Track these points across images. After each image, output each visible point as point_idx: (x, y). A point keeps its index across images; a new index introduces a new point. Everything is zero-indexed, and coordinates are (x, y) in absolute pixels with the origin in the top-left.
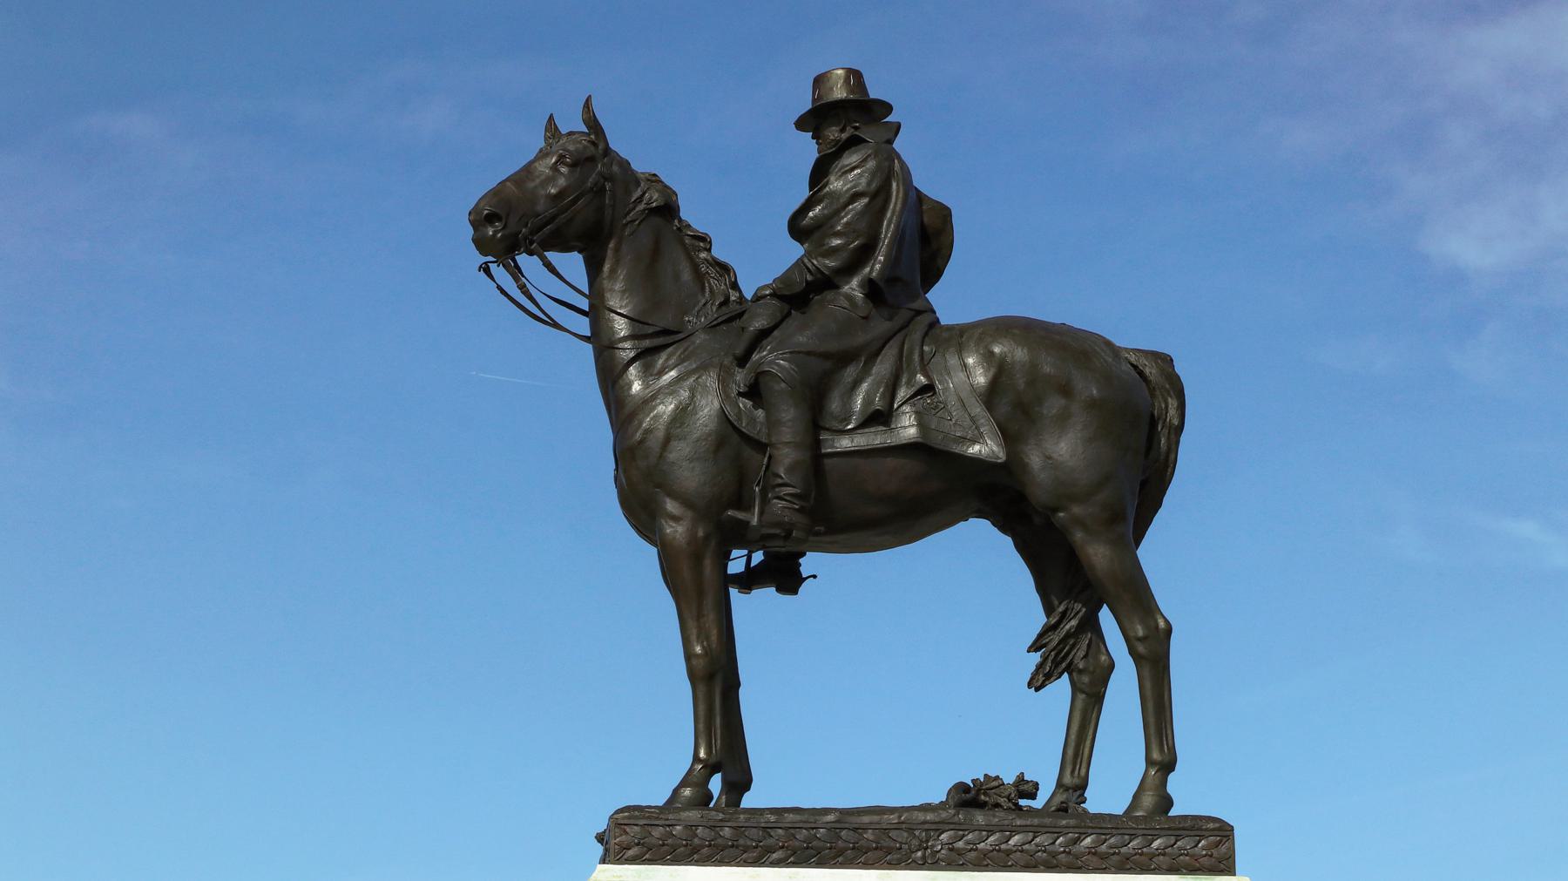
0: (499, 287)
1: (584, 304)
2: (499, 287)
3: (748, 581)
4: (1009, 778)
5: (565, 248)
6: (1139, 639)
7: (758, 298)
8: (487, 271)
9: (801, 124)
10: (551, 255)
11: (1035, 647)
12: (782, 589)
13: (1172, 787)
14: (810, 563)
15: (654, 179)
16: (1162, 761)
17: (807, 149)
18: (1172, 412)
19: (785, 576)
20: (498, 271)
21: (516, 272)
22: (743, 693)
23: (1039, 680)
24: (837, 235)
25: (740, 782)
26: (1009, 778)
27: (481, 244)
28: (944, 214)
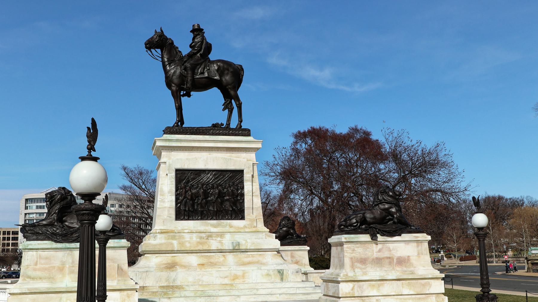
0: (149, 54)
2: (149, 54)
3: (184, 95)
4: (220, 123)
6: (238, 104)
7: (185, 56)
8: (147, 51)
9: (191, 32)
10: (156, 49)
11: (223, 105)
13: (242, 124)
14: (192, 93)
15: (170, 39)
17: (192, 35)
18: (242, 73)
21: (151, 52)
23: (224, 109)
24: (196, 47)
25: (183, 123)
26: (220, 123)
27: (146, 48)
28: (210, 45)
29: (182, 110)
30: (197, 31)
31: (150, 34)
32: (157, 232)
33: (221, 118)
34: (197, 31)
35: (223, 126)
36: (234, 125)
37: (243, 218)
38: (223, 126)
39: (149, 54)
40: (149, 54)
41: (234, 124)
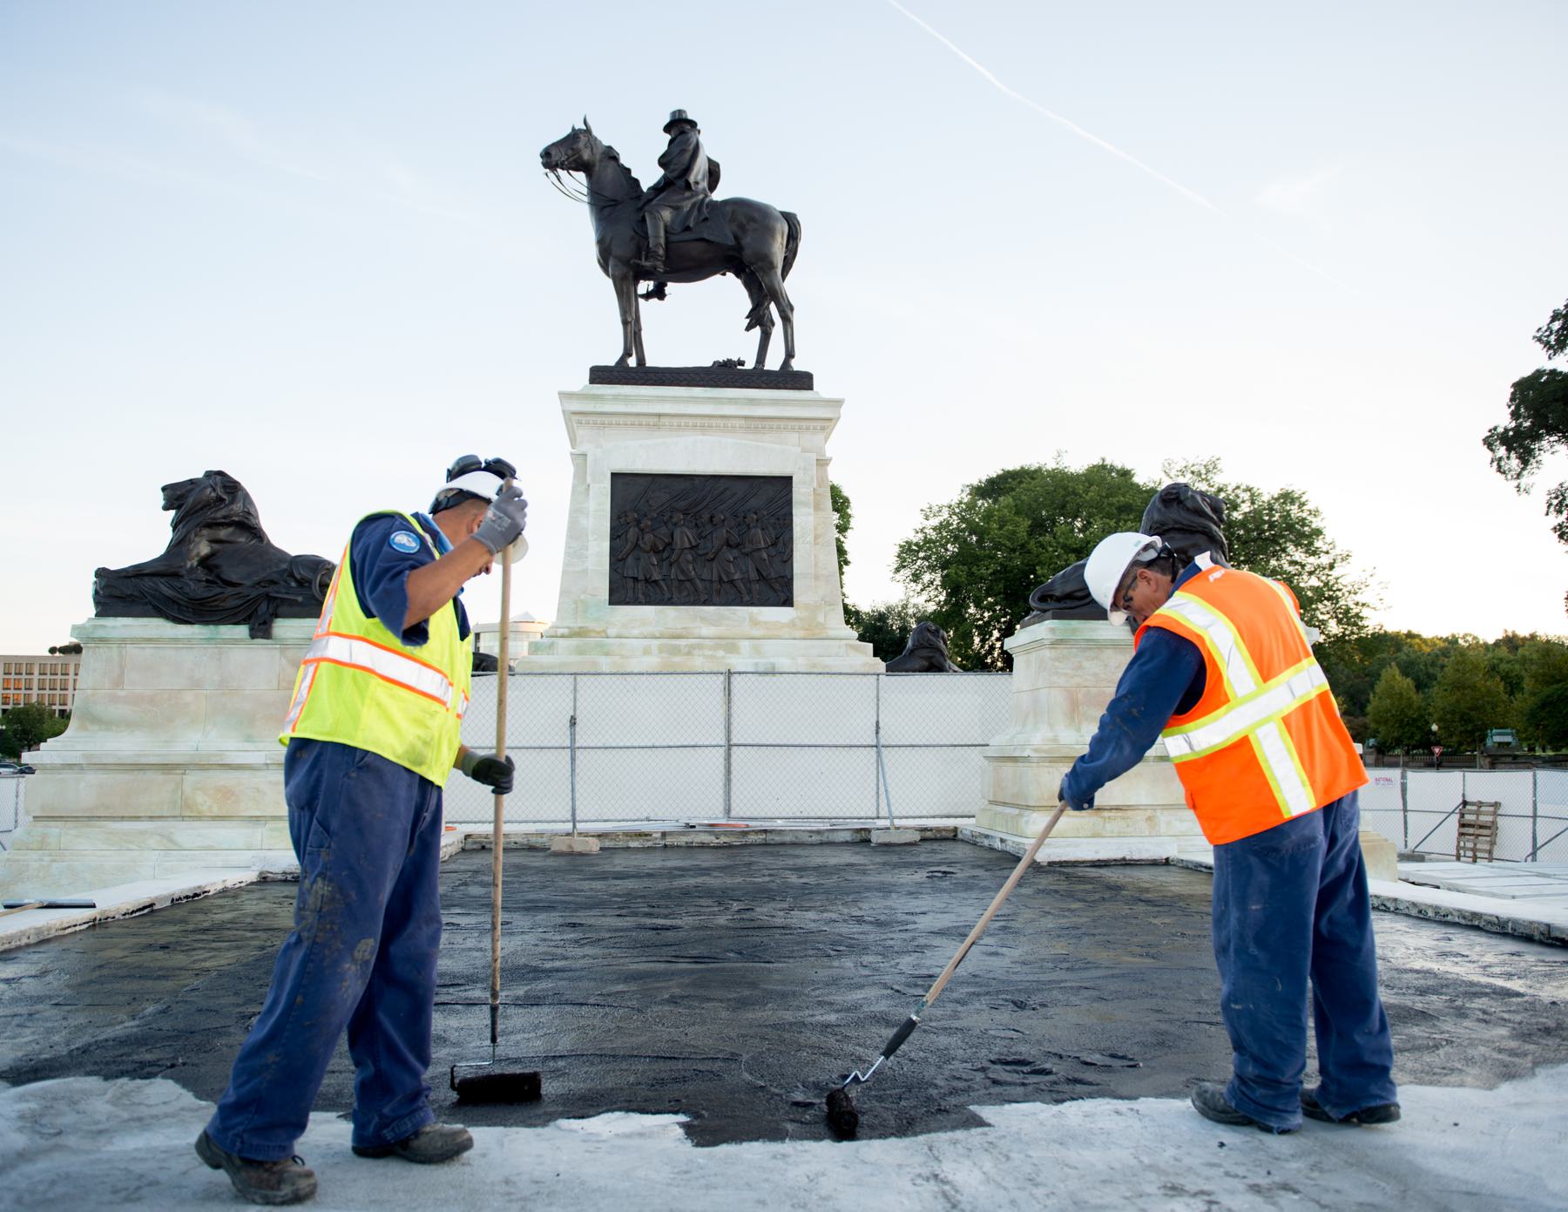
3: (648, 296)
11: (747, 317)
16: (790, 354)
19: (659, 293)
20: (551, 175)
21: (558, 178)
22: (643, 334)
23: (749, 328)
27: (546, 165)
28: (717, 165)
29: (640, 330)
30: (680, 127)
32: (559, 634)
33: (743, 347)
34: (680, 127)
37: (788, 601)
38: (743, 365)
41: (773, 362)
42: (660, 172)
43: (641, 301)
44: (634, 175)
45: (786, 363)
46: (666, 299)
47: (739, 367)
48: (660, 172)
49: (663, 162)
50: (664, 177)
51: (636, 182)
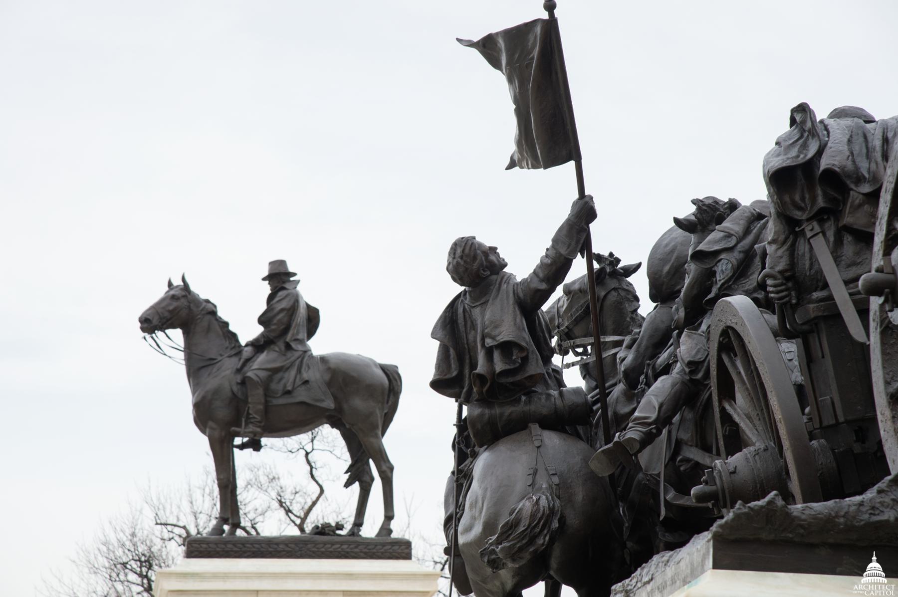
1: (183, 349)
3: (242, 447)
4: (333, 524)
5: (173, 327)
7: (247, 345)
8: (145, 338)
10: (168, 331)
11: (346, 472)
12: (254, 450)
13: (394, 525)
15: (208, 301)
19: (256, 445)
23: (348, 484)
24: (275, 324)
27: (143, 329)
31: (156, 293)
35: (341, 529)
36: (370, 530)
39: (151, 346)
40: (151, 346)
42: (260, 329)
43: (236, 451)
44: (232, 328)
45: (386, 530)
46: (262, 450)
47: (339, 532)
48: (260, 329)
49: (263, 320)
50: (262, 335)
51: (234, 336)
